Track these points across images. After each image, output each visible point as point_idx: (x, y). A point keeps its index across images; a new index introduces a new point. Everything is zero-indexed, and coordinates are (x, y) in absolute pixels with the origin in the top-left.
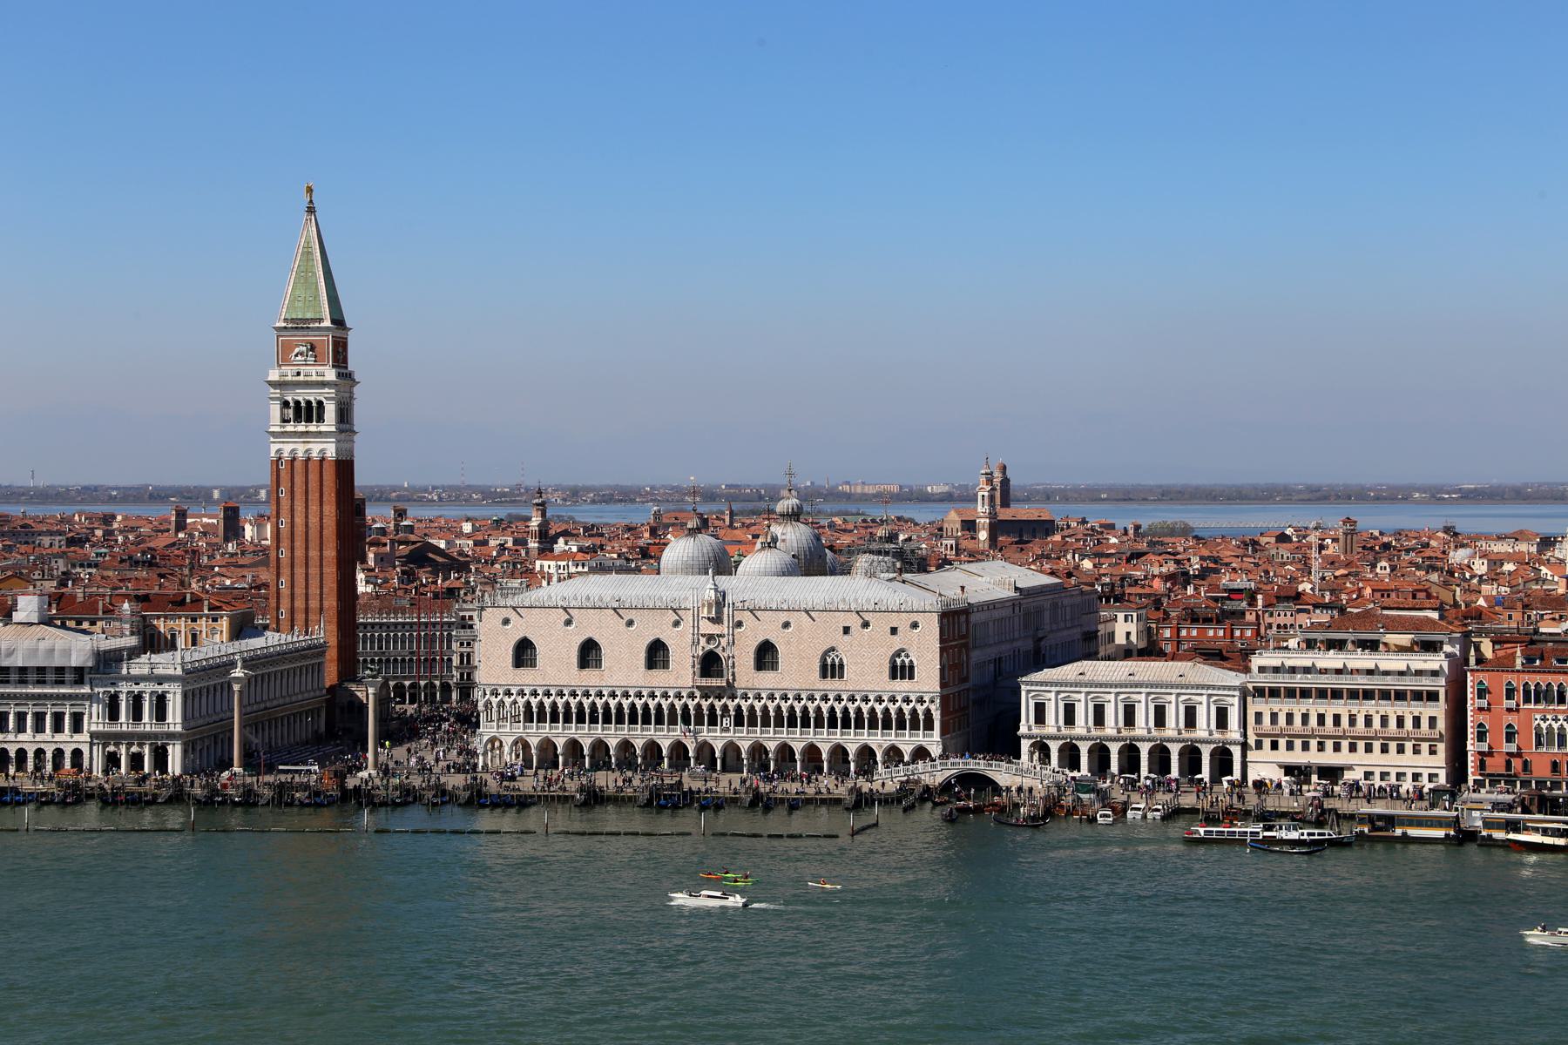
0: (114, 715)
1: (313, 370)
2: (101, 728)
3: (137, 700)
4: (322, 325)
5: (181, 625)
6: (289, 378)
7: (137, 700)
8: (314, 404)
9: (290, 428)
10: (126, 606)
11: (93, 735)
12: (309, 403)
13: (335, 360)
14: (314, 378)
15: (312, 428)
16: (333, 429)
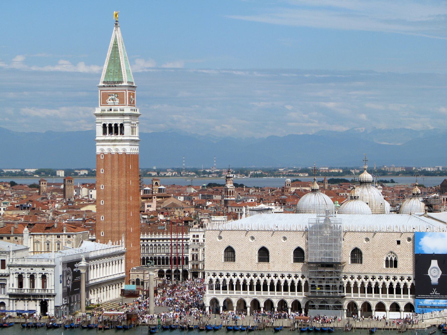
0: (21, 284)
1: (118, 108)
2: (14, 292)
3: (32, 277)
4: (123, 84)
5: (53, 239)
6: (106, 112)
7: (32, 277)
8: (119, 125)
9: (108, 137)
10: (26, 229)
11: (11, 295)
12: (116, 125)
13: (130, 102)
14: (119, 112)
15: (119, 137)
16: (128, 138)
